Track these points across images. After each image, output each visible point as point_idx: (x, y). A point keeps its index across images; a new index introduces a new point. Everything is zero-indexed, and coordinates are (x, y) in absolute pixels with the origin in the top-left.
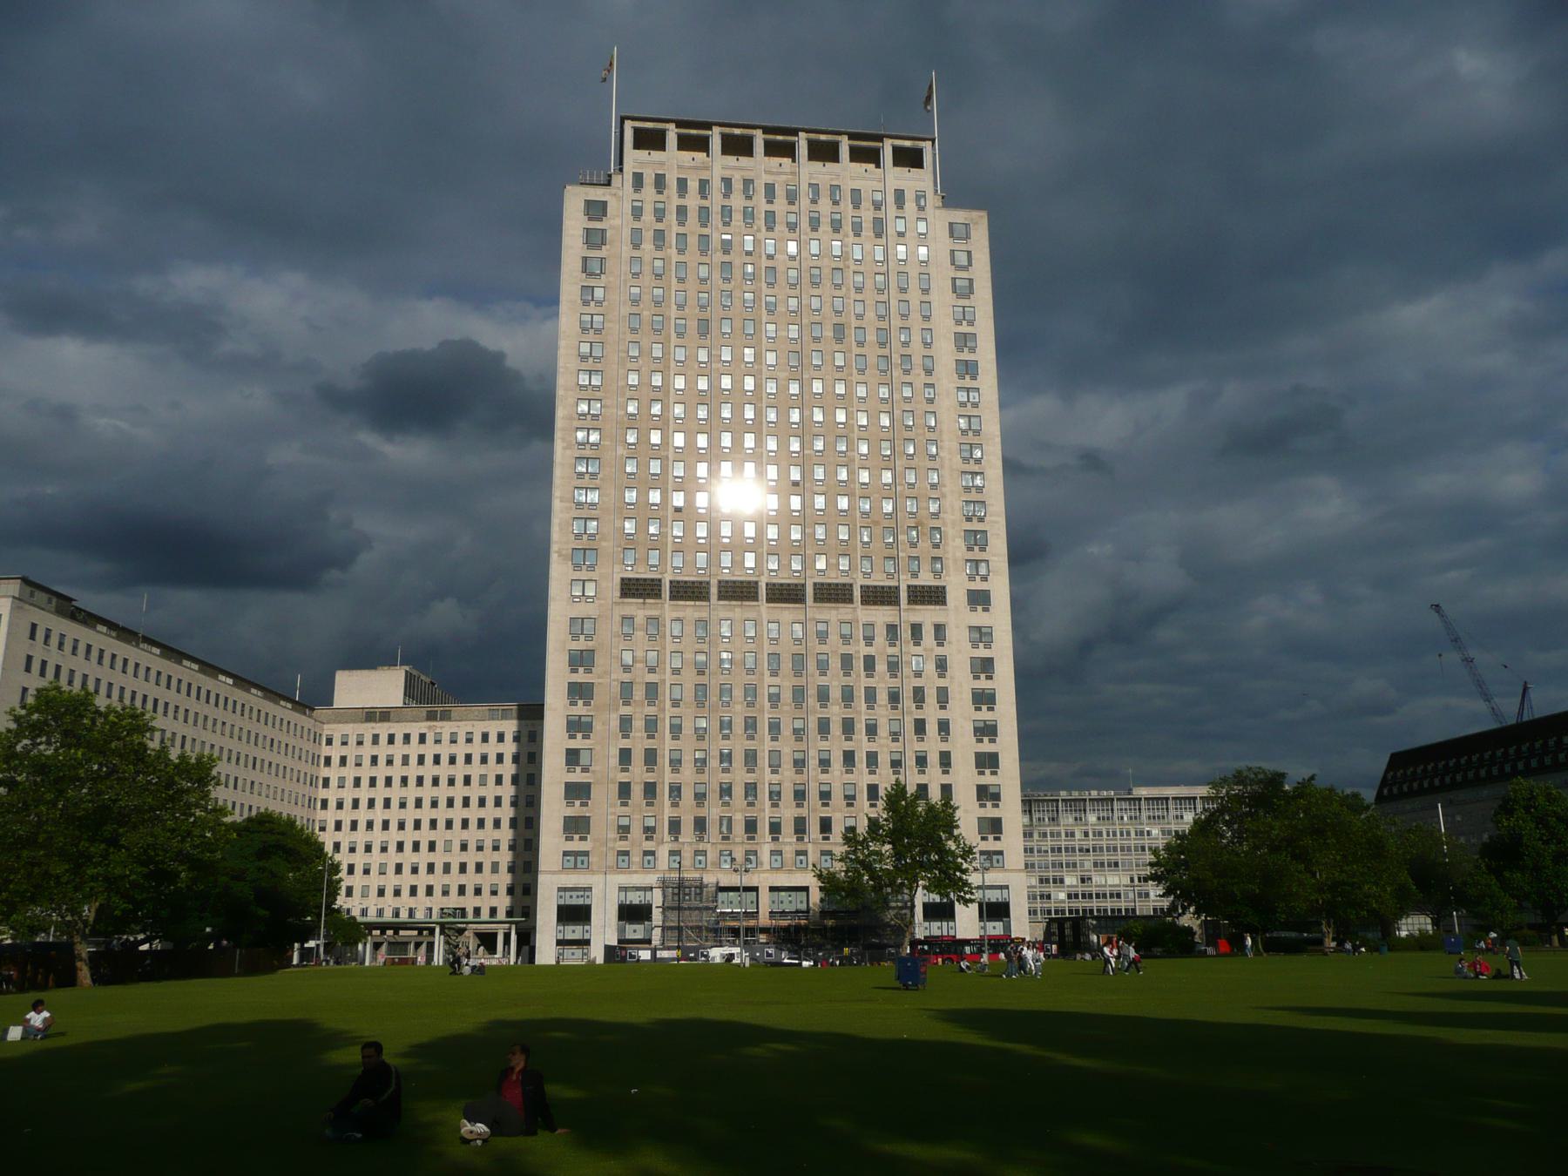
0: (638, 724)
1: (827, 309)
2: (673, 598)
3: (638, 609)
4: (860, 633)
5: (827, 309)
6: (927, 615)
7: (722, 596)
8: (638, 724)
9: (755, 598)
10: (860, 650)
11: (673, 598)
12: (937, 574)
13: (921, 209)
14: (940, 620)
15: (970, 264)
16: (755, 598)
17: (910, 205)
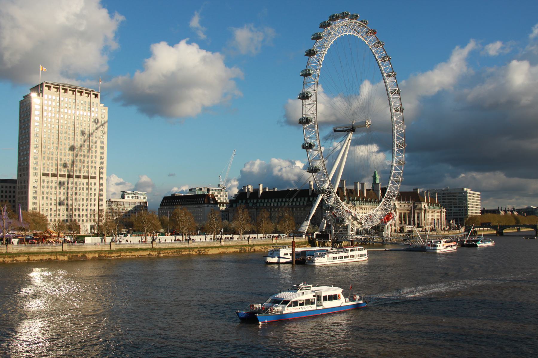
0: (45, 198)
1: (79, 125)
2: (51, 176)
3: (45, 178)
4: (82, 184)
5: (79, 125)
6: (93, 181)
7: (60, 176)
8: (45, 198)
9: (65, 177)
10: (82, 186)
11: (51, 176)
12: (95, 174)
13: (97, 106)
14: (95, 182)
15: (104, 117)
16: (65, 177)
17: (95, 106)
